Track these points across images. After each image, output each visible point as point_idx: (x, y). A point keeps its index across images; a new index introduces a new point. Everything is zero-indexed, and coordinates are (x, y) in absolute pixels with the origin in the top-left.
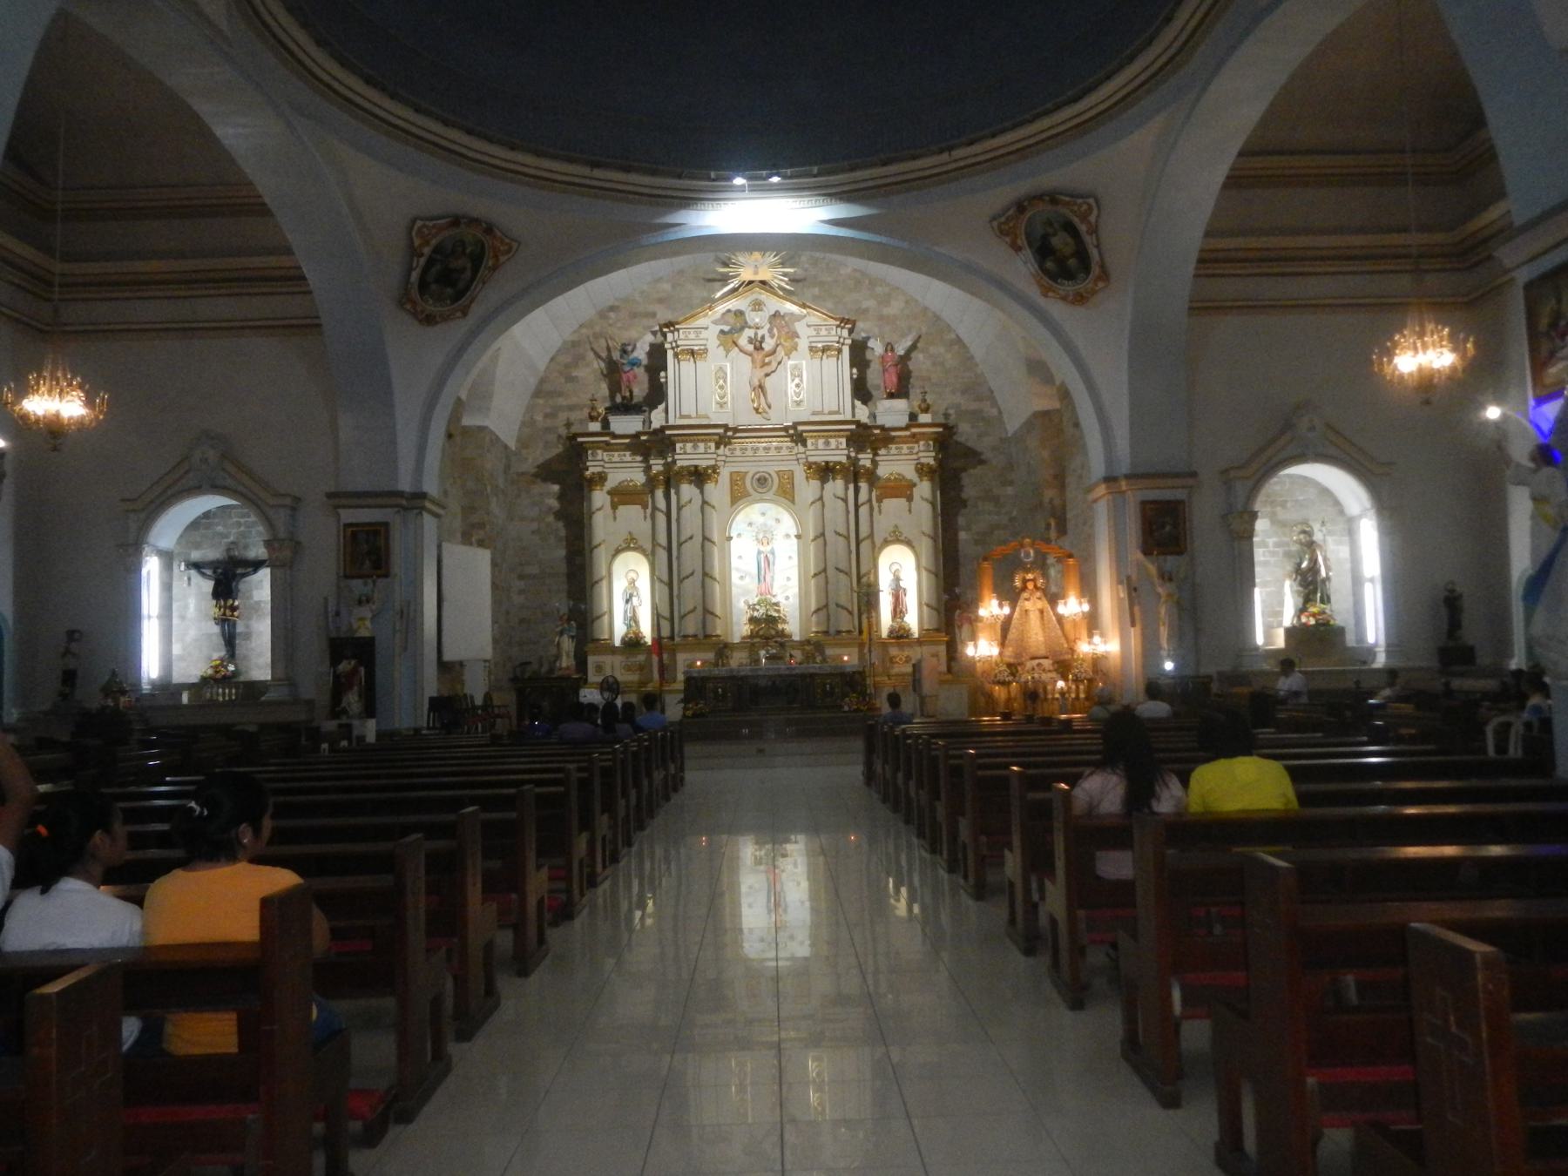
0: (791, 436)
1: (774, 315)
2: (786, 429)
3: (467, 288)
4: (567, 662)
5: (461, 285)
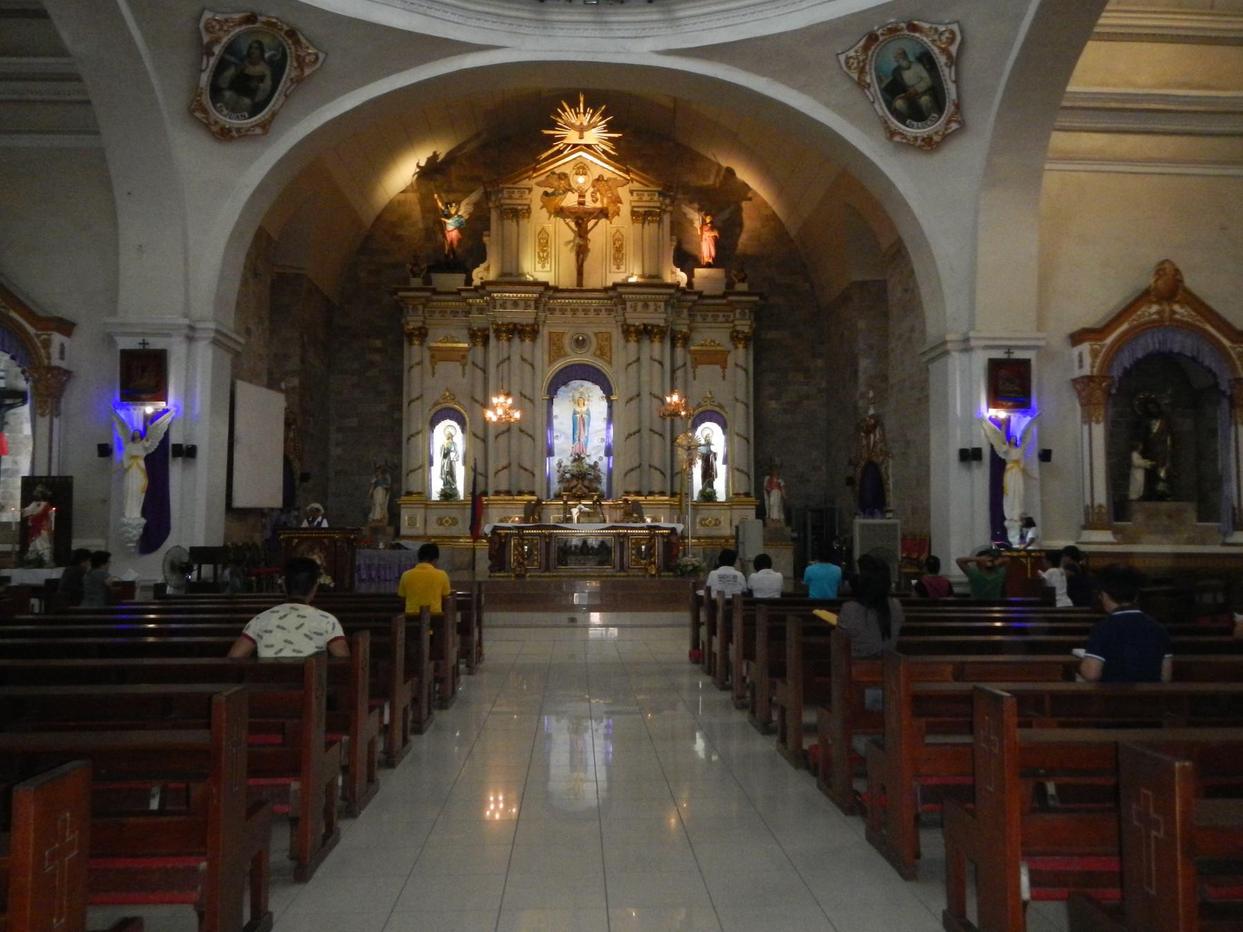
0: (611, 298)
1: (598, 180)
2: (606, 290)
4: (378, 512)
5: (260, 97)
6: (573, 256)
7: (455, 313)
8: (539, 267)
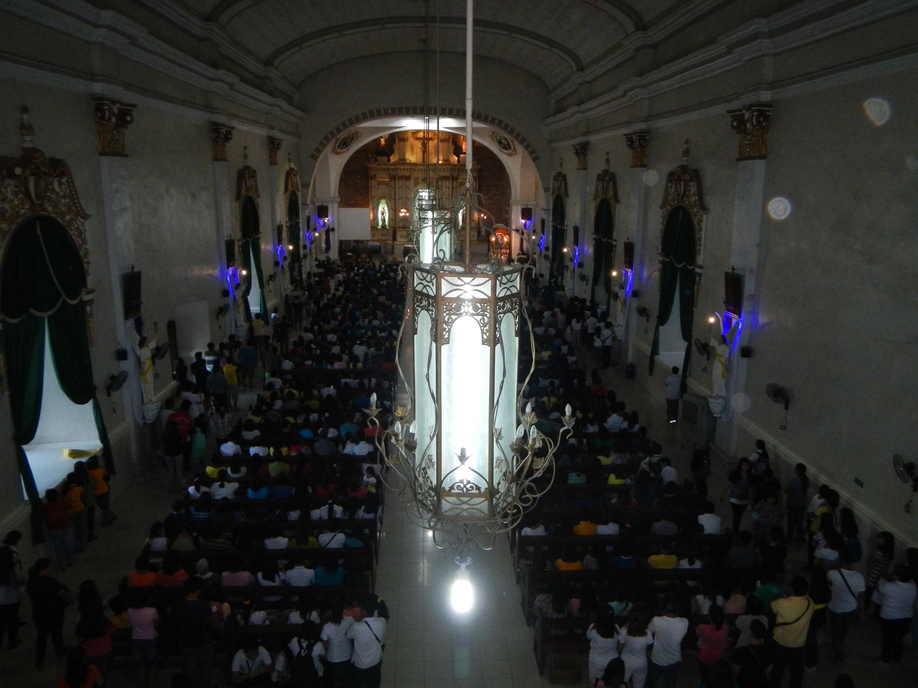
3: (349, 145)
6: (421, 153)
7: (384, 169)
8: (411, 156)
